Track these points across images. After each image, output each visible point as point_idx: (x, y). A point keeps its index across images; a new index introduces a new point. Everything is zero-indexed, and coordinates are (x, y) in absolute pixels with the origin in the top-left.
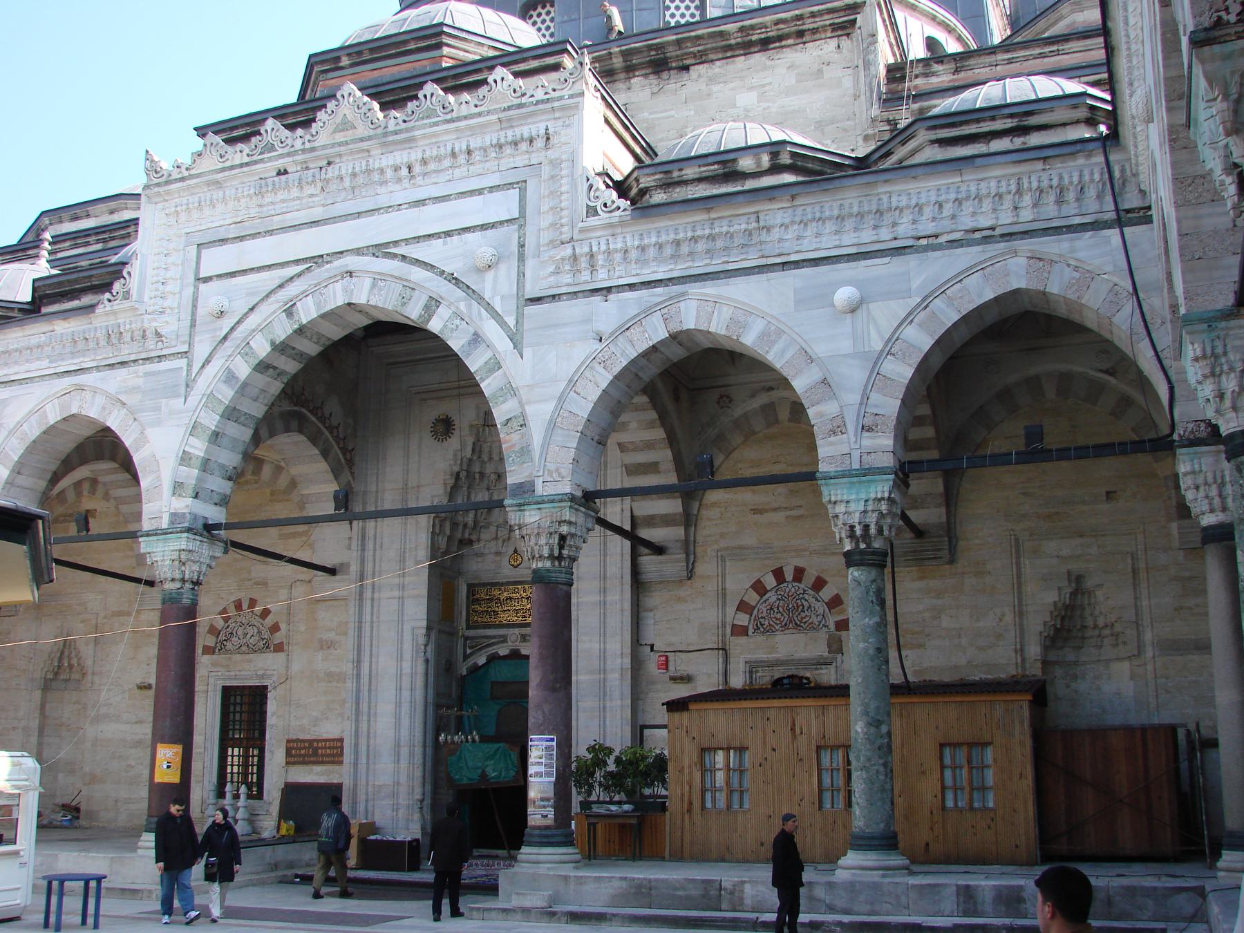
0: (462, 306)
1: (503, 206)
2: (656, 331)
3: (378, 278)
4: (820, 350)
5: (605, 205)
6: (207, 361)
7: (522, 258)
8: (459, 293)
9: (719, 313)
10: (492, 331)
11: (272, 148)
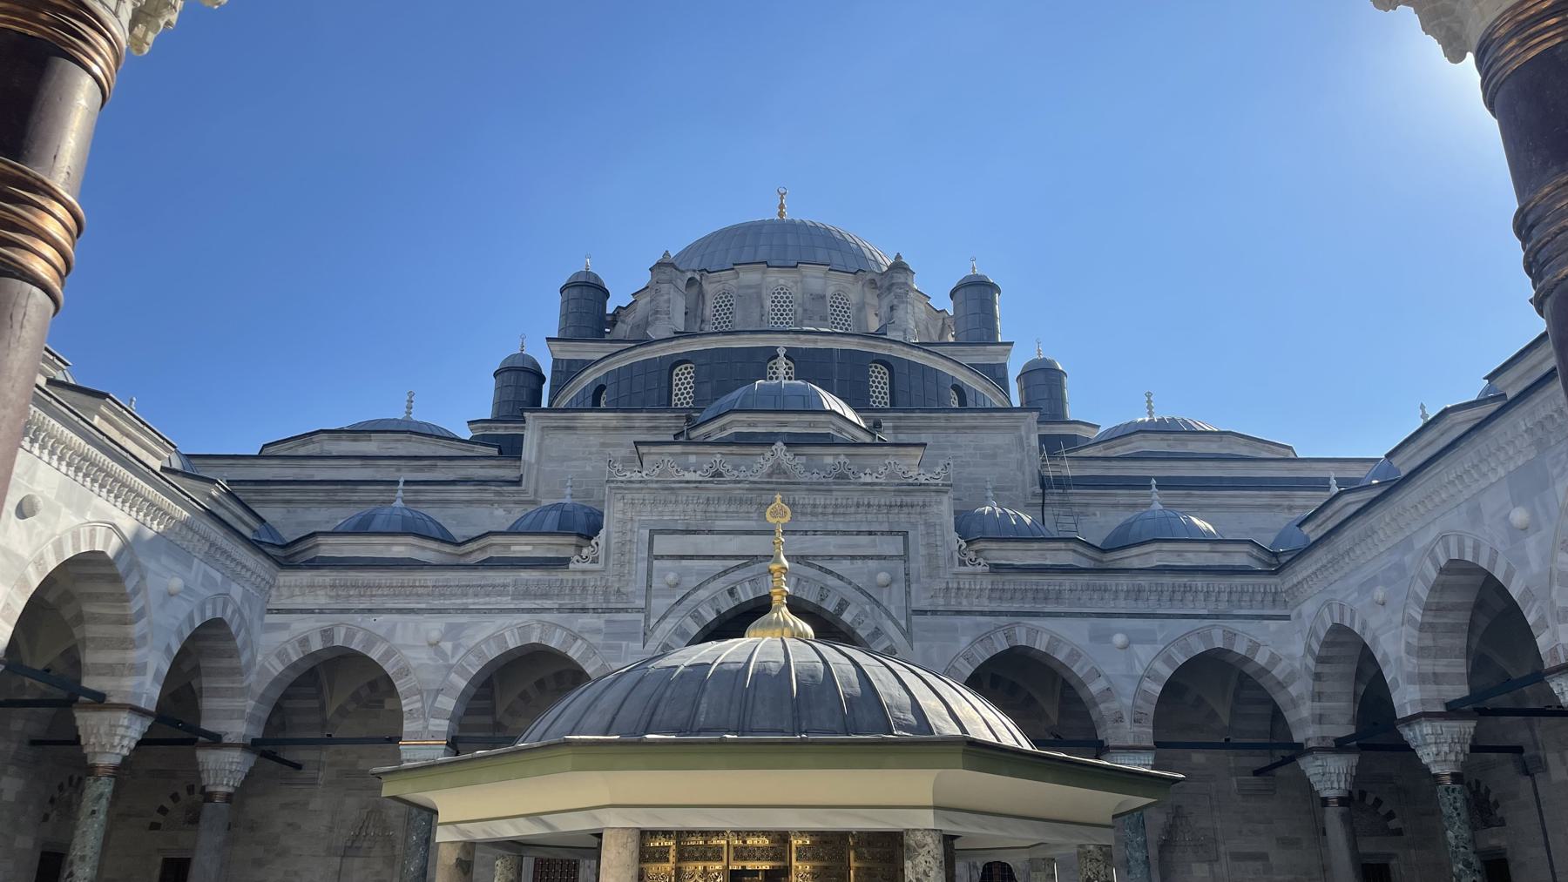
2: (1001, 645)
4: (1106, 670)
6: (664, 617)
7: (908, 582)
8: (865, 599)
10: (889, 627)
11: (721, 475)
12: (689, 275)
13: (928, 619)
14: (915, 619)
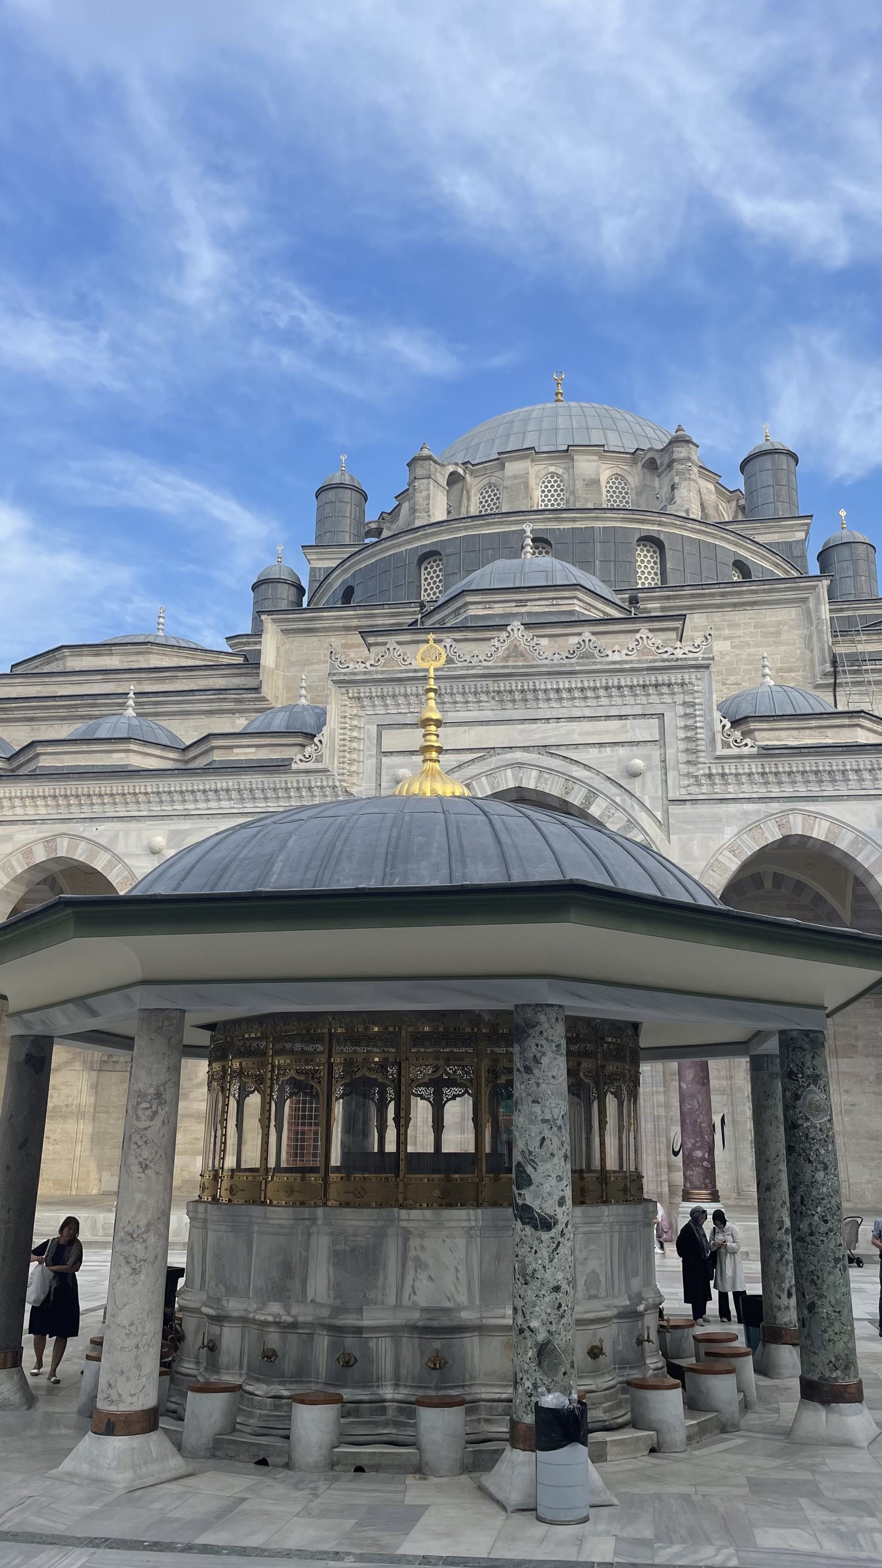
0: (618, 799)
2: (773, 834)
3: (542, 769)
5: (736, 741)
7: (665, 768)
9: (820, 825)
10: (643, 818)
12: (451, 469)
13: (688, 808)
14: (674, 809)
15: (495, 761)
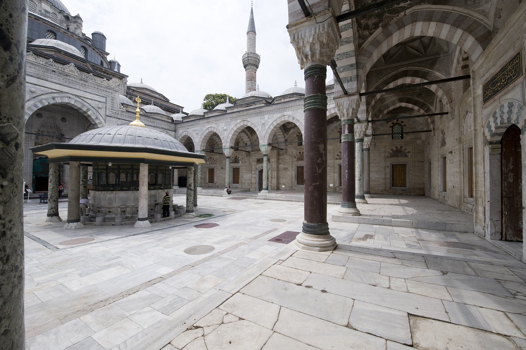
1: (103, 100)
3: (76, 101)
7: (106, 109)
10: (100, 117)
11: (52, 66)
15: (64, 95)
